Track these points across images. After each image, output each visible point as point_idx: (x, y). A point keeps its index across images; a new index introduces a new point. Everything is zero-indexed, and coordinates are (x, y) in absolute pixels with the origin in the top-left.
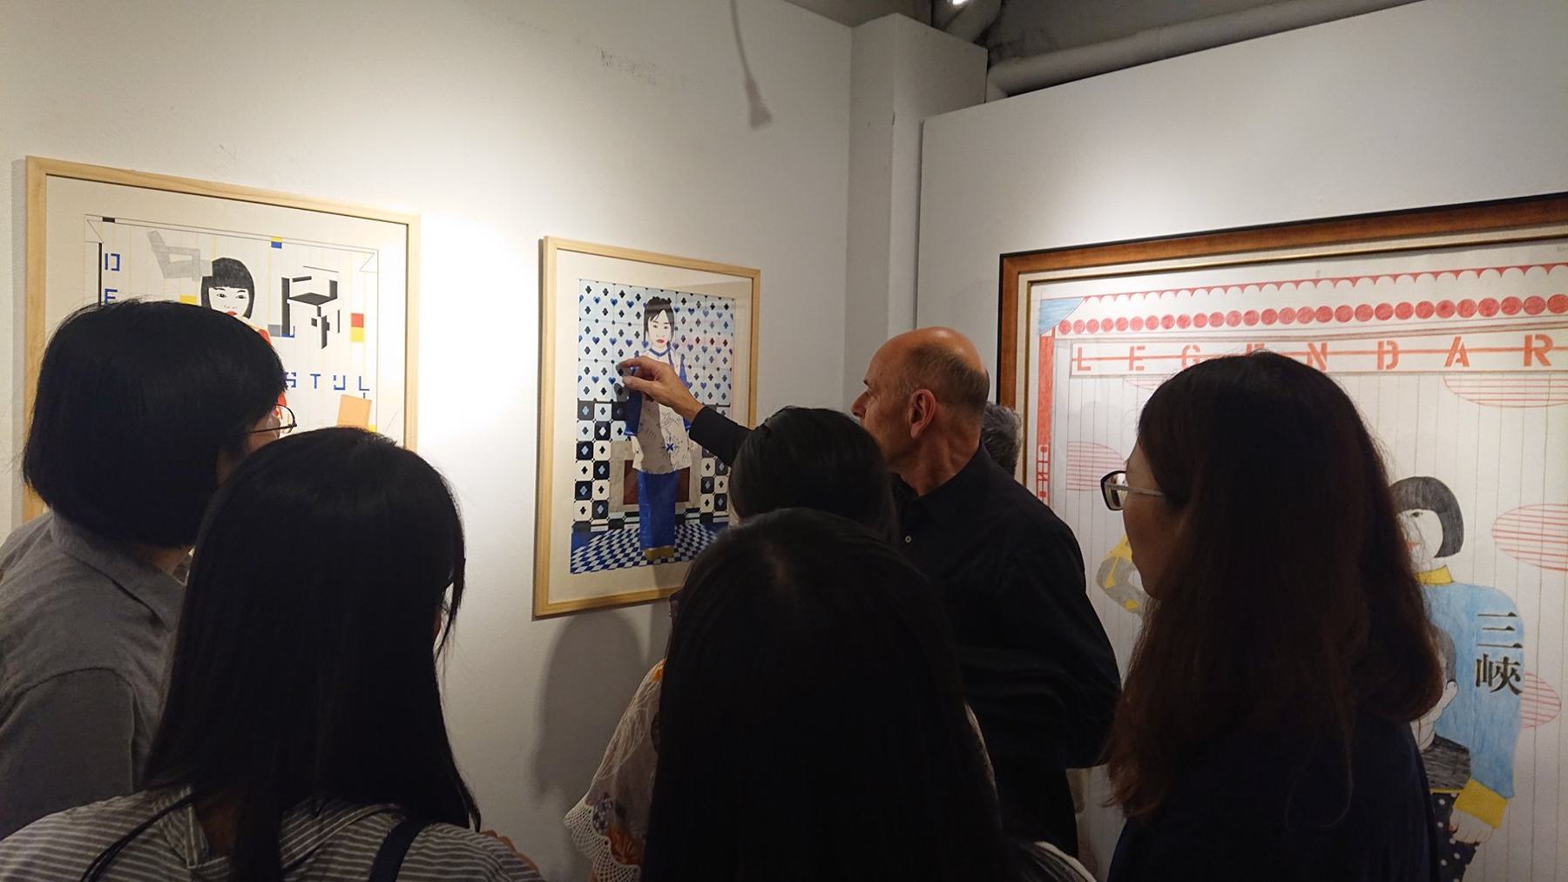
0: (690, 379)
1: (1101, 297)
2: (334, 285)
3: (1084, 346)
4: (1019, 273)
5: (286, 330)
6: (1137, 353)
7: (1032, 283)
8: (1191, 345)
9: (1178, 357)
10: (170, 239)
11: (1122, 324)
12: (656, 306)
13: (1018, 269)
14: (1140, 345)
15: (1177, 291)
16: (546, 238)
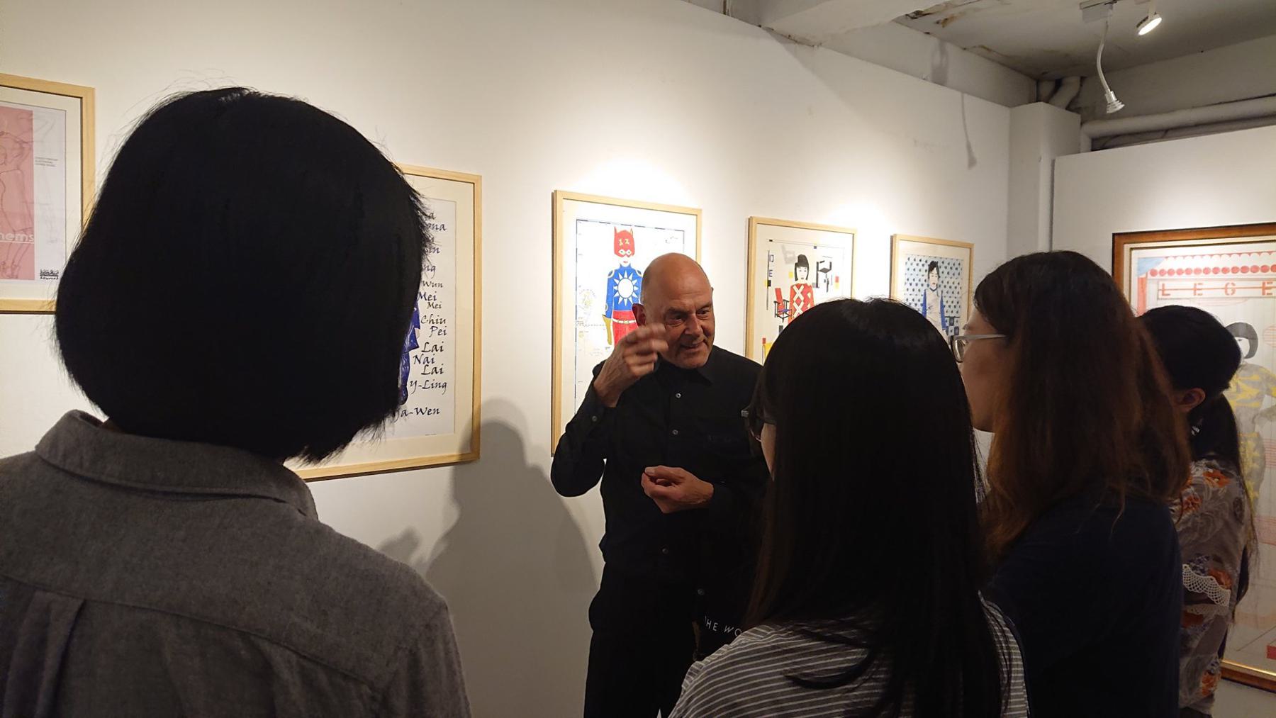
0: (944, 303)
1: (1175, 257)
2: (831, 263)
3: (1165, 283)
4: (1125, 243)
5: (817, 286)
6: (1198, 287)
7: (1132, 249)
8: (1230, 282)
9: (1222, 289)
10: (788, 248)
11: (1188, 271)
12: (933, 265)
13: (1125, 241)
14: (1201, 282)
15: (1221, 255)
16: (895, 235)
